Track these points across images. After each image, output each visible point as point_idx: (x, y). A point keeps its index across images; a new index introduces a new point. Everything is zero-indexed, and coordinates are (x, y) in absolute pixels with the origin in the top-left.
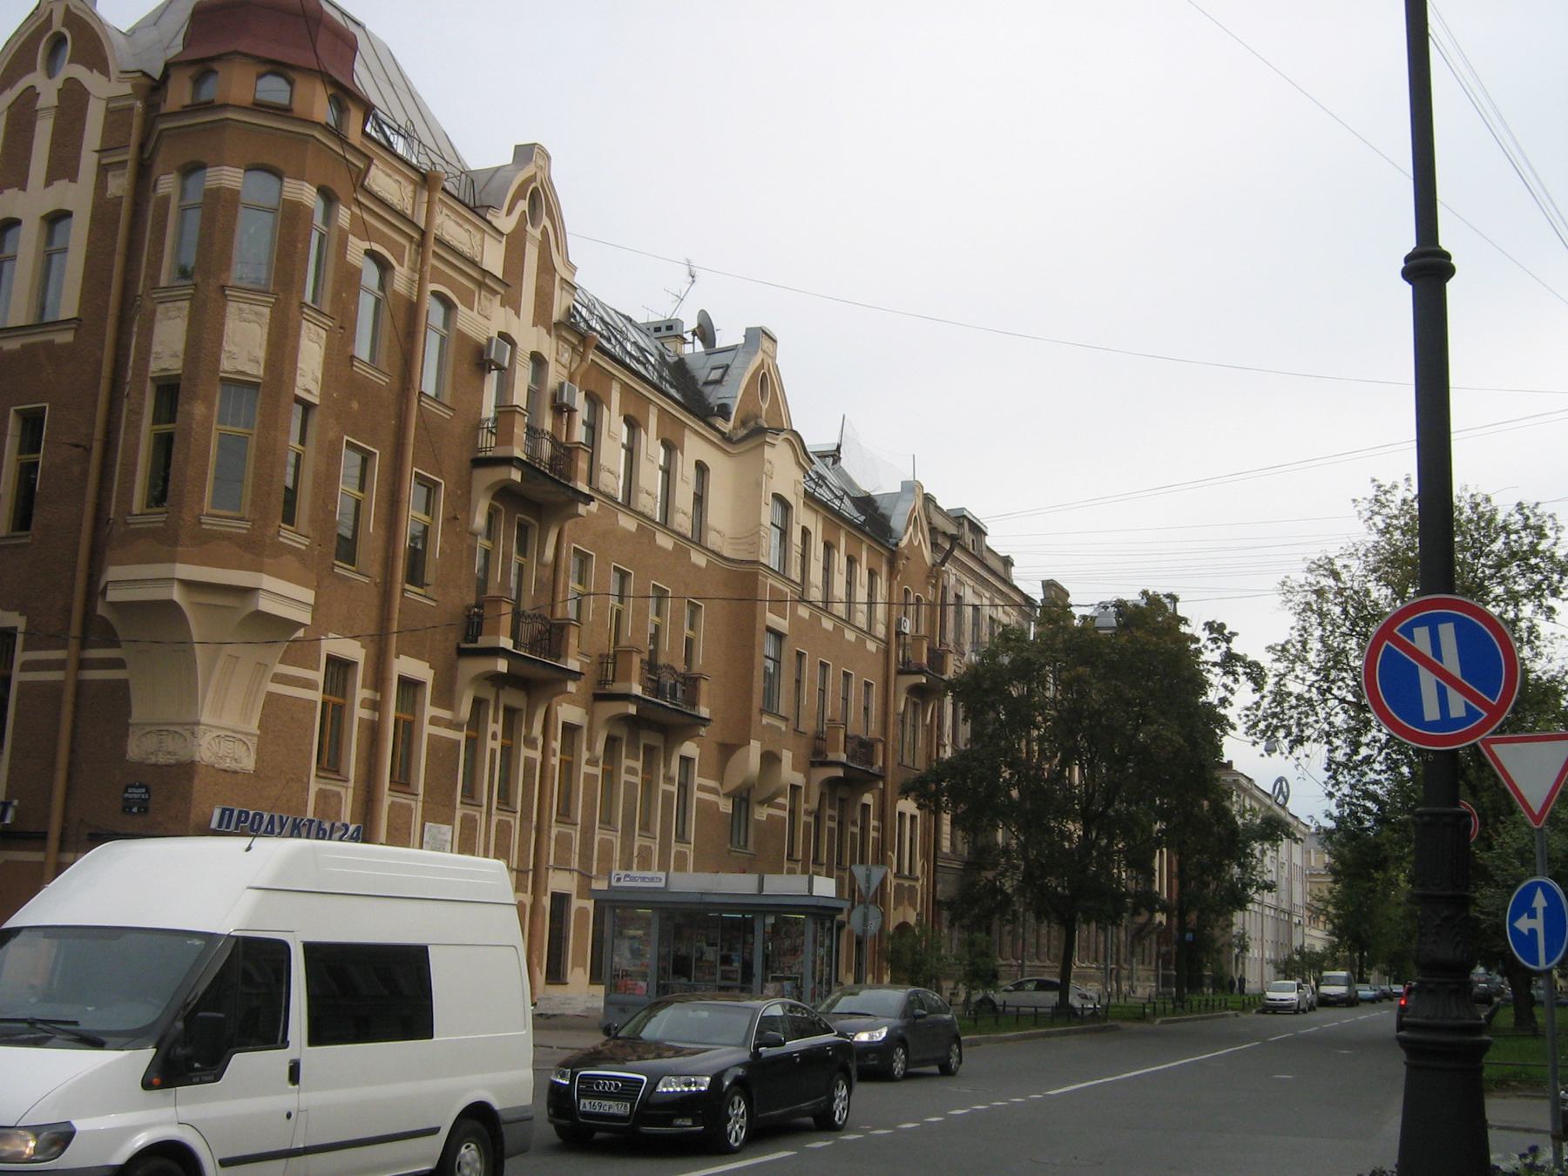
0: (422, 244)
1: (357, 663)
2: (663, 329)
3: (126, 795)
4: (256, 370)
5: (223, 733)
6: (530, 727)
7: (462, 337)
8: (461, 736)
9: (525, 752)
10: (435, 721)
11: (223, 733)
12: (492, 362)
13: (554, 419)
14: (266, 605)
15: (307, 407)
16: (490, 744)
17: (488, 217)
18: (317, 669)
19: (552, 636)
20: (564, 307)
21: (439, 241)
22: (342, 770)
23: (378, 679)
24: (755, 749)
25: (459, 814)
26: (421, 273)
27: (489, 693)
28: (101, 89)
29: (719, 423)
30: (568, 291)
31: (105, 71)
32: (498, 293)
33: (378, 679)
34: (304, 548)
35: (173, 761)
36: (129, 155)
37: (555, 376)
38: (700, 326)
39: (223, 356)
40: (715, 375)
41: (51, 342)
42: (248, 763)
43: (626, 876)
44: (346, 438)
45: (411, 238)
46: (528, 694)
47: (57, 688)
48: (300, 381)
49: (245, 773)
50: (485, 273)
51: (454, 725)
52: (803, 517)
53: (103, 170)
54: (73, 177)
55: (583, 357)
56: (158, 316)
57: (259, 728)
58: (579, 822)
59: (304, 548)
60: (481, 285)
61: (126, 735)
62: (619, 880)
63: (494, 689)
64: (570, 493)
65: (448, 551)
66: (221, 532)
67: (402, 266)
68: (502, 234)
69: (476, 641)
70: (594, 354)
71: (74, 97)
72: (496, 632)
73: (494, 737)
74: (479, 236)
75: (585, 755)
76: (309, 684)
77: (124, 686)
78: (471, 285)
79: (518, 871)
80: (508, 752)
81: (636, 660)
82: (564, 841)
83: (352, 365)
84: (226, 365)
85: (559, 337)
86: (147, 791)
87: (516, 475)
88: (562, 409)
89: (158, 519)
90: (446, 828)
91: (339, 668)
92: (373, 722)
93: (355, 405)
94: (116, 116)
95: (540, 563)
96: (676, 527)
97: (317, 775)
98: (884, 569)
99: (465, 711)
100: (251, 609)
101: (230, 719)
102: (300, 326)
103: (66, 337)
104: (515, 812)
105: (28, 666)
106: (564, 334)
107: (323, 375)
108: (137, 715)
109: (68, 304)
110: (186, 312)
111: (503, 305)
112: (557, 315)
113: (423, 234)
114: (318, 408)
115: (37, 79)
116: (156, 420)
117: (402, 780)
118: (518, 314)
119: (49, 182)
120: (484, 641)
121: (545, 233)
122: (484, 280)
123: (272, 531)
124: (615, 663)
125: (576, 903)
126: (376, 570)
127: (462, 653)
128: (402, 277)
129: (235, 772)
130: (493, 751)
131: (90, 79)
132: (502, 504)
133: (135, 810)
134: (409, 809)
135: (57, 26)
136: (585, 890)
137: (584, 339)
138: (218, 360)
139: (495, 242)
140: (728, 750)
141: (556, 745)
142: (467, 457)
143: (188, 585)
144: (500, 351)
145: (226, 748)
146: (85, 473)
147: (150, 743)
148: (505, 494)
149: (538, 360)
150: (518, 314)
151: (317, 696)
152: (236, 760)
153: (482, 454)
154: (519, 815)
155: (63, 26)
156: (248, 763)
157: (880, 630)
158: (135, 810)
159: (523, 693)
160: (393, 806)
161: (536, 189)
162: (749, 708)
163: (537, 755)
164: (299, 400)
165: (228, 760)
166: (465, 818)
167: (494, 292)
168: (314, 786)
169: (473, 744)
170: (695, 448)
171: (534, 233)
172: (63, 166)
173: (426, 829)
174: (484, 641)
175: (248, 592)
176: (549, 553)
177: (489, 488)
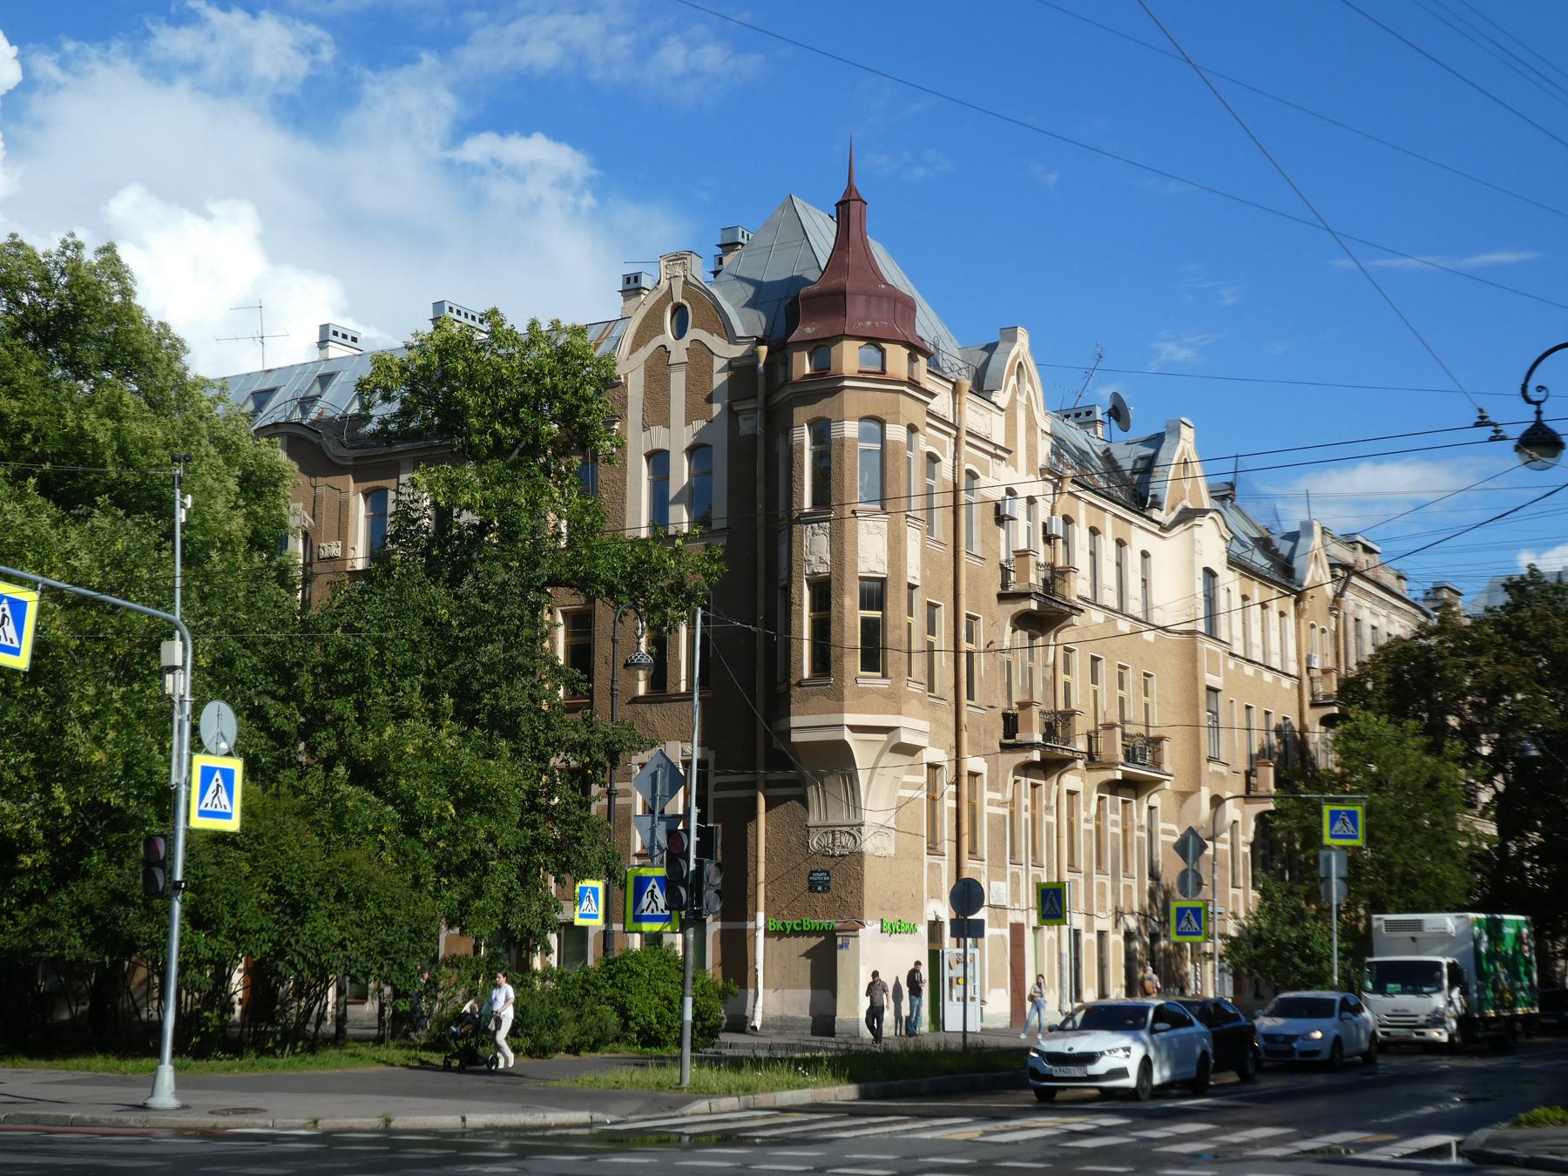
0: (957, 440)
2: (1083, 414)
10: (991, 802)
15: (912, 587)
17: (993, 399)
21: (969, 433)
24: (1205, 795)
25: (1009, 872)
29: (1156, 514)
32: (1002, 459)
38: (1114, 407)
42: (891, 851)
50: (997, 446)
51: (1002, 804)
58: (986, 857)
68: (1002, 410)
87: (1034, 605)
90: (1002, 884)
96: (1130, 612)
100: (895, 742)
105: (718, 787)
113: (957, 429)
118: (1016, 470)
121: (1028, 398)
127: (1004, 747)
130: (1026, 820)
133: (820, 888)
138: (856, 565)
140: (1184, 796)
143: (855, 729)
149: (1031, 500)
150: (1016, 470)
157: (1293, 669)
158: (820, 888)
162: (1198, 760)
166: (1012, 874)
170: (1140, 539)
171: (1022, 399)
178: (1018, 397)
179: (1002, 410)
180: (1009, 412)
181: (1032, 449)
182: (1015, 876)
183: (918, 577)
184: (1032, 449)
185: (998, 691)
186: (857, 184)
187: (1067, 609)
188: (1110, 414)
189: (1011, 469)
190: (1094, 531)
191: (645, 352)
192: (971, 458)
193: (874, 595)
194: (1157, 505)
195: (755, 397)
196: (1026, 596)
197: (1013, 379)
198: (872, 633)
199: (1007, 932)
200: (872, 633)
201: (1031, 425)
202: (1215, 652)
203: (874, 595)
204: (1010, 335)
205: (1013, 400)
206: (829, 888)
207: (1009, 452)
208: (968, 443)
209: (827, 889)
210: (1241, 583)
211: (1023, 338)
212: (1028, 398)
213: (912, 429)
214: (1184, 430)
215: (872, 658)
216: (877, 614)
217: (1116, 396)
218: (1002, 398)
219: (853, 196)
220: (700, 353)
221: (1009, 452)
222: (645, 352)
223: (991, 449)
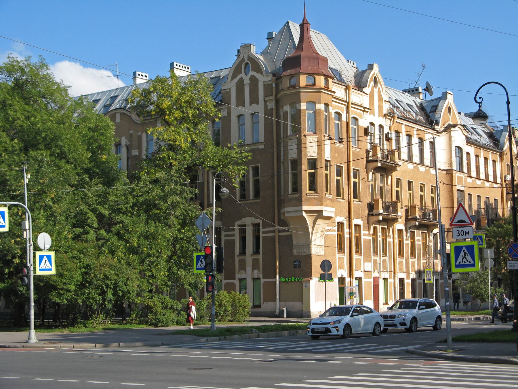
2: (415, 90)
8: (371, 238)
9: (388, 240)
19: (392, 207)
21: (352, 104)
28: (263, 79)
29: (436, 127)
31: (262, 73)
32: (367, 112)
36: (273, 98)
37: (386, 130)
38: (427, 87)
40: (433, 109)
41: (258, 148)
46: (387, 223)
47: (273, 238)
50: (364, 108)
51: (369, 235)
52: (467, 148)
53: (265, 102)
54: (257, 103)
61: (292, 249)
68: (367, 94)
73: (380, 237)
75: (405, 238)
77: (291, 236)
78: (361, 112)
81: (417, 209)
82: (401, 262)
86: (300, 262)
87: (379, 164)
88: (388, 139)
89: (296, 196)
90: (370, 264)
91: (340, 225)
93: (337, 155)
94: (267, 87)
98: (498, 159)
103: (262, 147)
109: (262, 138)
112: (385, 111)
113: (348, 103)
115: (242, 75)
116: (292, 170)
117: (358, 251)
118: (374, 115)
119: (251, 105)
121: (379, 89)
122: (365, 110)
124: (411, 210)
125: (406, 281)
126: (347, 199)
130: (380, 241)
131: (258, 76)
135: (246, 60)
136: (408, 278)
141: (396, 236)
144: (371, 128)
145: (318, 250)
146: (273, 183)
149: (381, 127)
150: (374, 115)
151: (336, 233)
157: (499, 181)
161: (375, 77)
163: (391, 240)
167: (367, 112)
171: (376, 90)
172: (254, 100)
178: (375, 89)
179: (367, 94)
180: (371, 96)
181: (380, 108)
182: (375, 261)
183: (330, 157)
184: (380, 108)
185: (367, 195)
186: (306, 17)
187: (394, 165)
188: (425, 90)
189: (372, 115)
190: (409, 136)
191: (236, 80)
192: (354, 112)
193: (313, 163)
194: (437, 124)
195: (272, 95)
196: (377, 161)
197: (372, 83)
198: (313, 177)
199: (372, 280)
200: (313, 177)
201: (380, 98)
202: (461, 177)
203: (313, 163)
204: (371, 67)
205: (372, 91)
206: (300, 267)
207: (370, 109)
208: (352, 107)
209: (300, 267)
210: (475, 150)
211: (376, 67)
212: (379, 89)
213: (327, 105)
214: (448, 95)
215: (313, 188)
216: (313, 171)
217: (427, 83)
218: (367, 90)
219: (305, 22)
220: (254, 81)
221: (370, 109)
222: (236, 80)
223: (362, 109)
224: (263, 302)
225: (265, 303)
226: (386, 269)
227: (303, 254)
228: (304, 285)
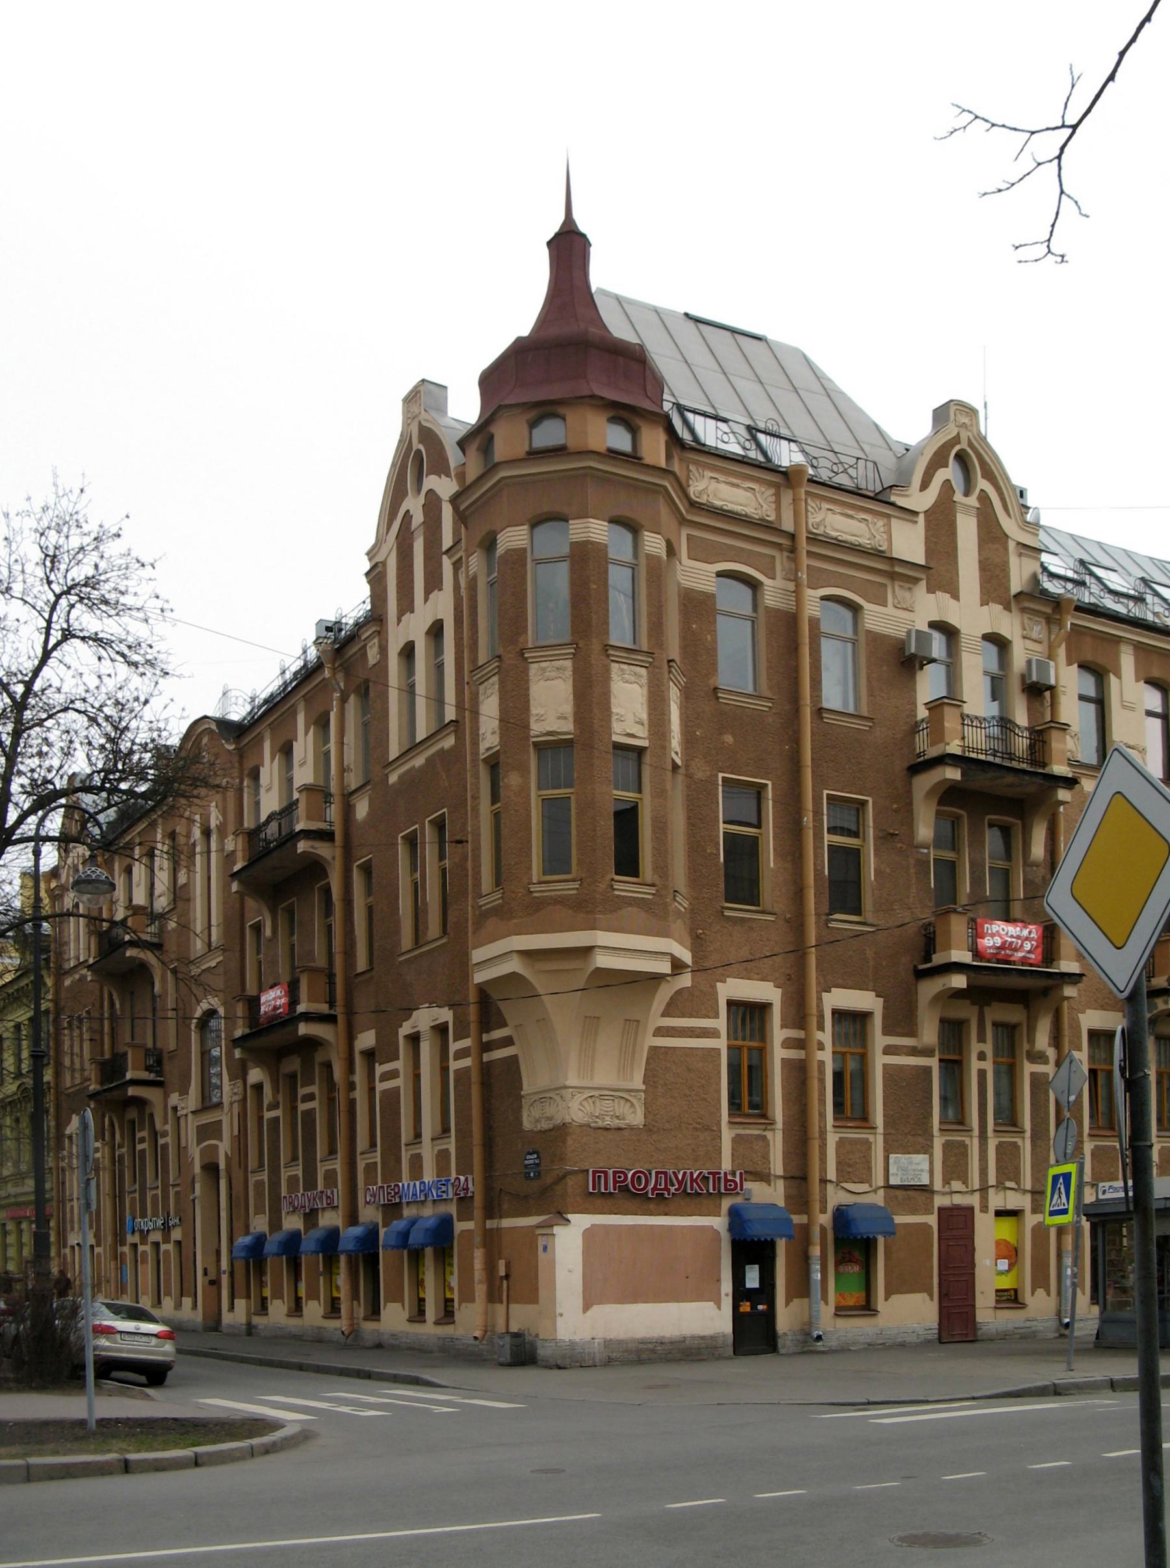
0: (793, 550)
1: (771, 1004)
3: (526, 1162)
4: (567, 727)
5: (596, 1093)
6: (1031, 1040)
7: (875, 638)
8: (933, 1063)
10: (888, 1050)
11: (596, 1093)
12: (913, 657)
13: (1029, 702)
14: (602, 961)
16: (975, 1065)
18: (716, 1016)
20: (1026, 575)
22: (770, 1114)
23: (798, 1014)
26: (796, 580)
27: (967, 1011)
30: (1029, 556)
33: (798, 1014)
34: (650, 897)
35: (551, 1126)
37: (1019, 656)
39: (532, 720)
42: (637, 1118)
43: (1110, 1187)
44: (721, 775)
45: (778, 546)
46: (1027, 1007)
48: (617, 727)
49: (631, 1128)
51: (914, 1051)
55: (1060, 623)
56: (481, 698)
57: (644, 1083)
59: (650, 897)
60: (893, 576)
62: (1104, 1192)
63: (976, 1009)
64: (1039, 781)
65: (888, 870)
66: (551, 897)
67: (773, 578)
69: (930, 961)
70: (1074, 617)
71: (432, 504)
72: (948, 947)
74: (880, 523)
76: (713, 1033)
79: (1033, 1193)
80: (1009, 1072)
83: (718, 698)
84: (536, 728)
85: (1023, 610)
86: (538, 1157)
92: (801, 1061)
93: (729, 739)
95: (1027, 863)
97: (730, 1122)
99: (929, 1034)
100: (592, 968)
101: (605, 1076)
102: (608, 671)
104: (1023, 1132)
106: (1027, 604)
107: (650, 715)
108: (527, 1088)
110: (497, 686)
111: (930, 590)
112: (1016, 585)
114: (648, 752)
118: (956, 597)
120: (938, 959)
123: (602, 886)
127: (921, 975)
128: (774, 591)
129: (620, 1129)
130: (982, 1074)
132: (961, 808)
133: (532, 1175)
134: (867, 1144)
137: (1057, 603)
139: (910, 524)
142: (899, 765)
143: (528, 955)
147: (536, 1112)
148: (949, 795)
150: (956, 597)
151: (721, 1044)
152: (617, 1117)
153: (922, 759)
154: (1028, 1134)
155: (420, 442)
156: (637, 1118)
158: (532, 1175)
159: (1021, 1006)
160: (841, 1143)
164: (618, 747)
165: (607, 1118)
166: (947, 1146)
168: (727, 1135)
169: (953, 1067)
173: (891, 1161)
174: (938, 959)
175: (587, 951)
176: (1038, 850)
177: (930, 793)
206: (539, 1174)
224: (460, 1305)
225: (464, 1305)
226: (1017, 1178)
227: (545, 1125)
228: (541, 1242)
